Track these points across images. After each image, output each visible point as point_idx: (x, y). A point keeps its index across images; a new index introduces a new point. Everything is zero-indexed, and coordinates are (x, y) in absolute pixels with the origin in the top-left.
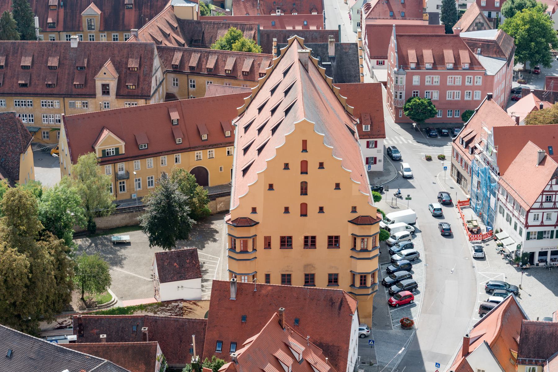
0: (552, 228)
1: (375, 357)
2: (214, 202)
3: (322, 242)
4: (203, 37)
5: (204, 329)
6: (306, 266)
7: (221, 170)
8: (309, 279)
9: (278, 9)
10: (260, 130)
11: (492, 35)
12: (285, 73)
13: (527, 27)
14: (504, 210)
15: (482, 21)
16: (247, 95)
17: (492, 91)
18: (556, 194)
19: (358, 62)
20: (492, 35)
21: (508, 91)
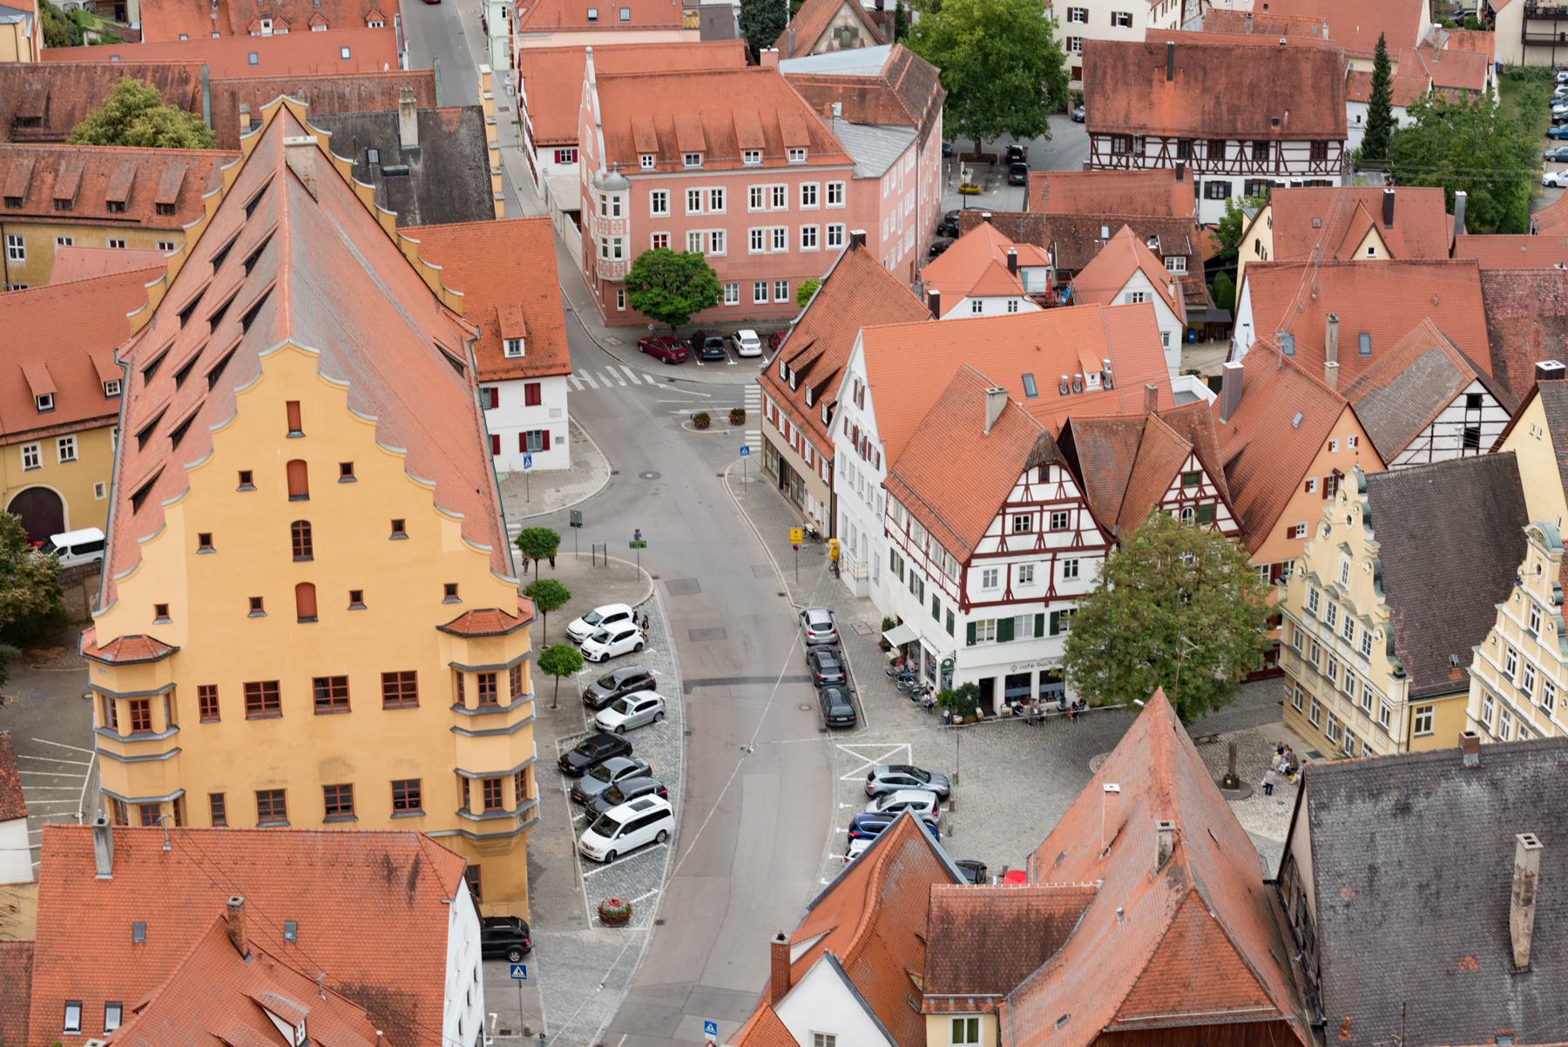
0: (1039, 608)
1: (540, 1011)
2: (80, 589)
3: (366, 692)
4: (47, 108)
5: (26, 969)
6: (326, 764)
7: (99, 493)
8: (339, 801)
9: (266, 16)
10: (181, 376)
11: (872, 60)
12: (250, 208)
13: (979, 32)
14: (902, 562)
15: (852, 22)
16: (150, 274)
17: (874, 217)
18: (1041, 512)
19: (487, 160)
20: (872, 60)
21: (927, 221)
